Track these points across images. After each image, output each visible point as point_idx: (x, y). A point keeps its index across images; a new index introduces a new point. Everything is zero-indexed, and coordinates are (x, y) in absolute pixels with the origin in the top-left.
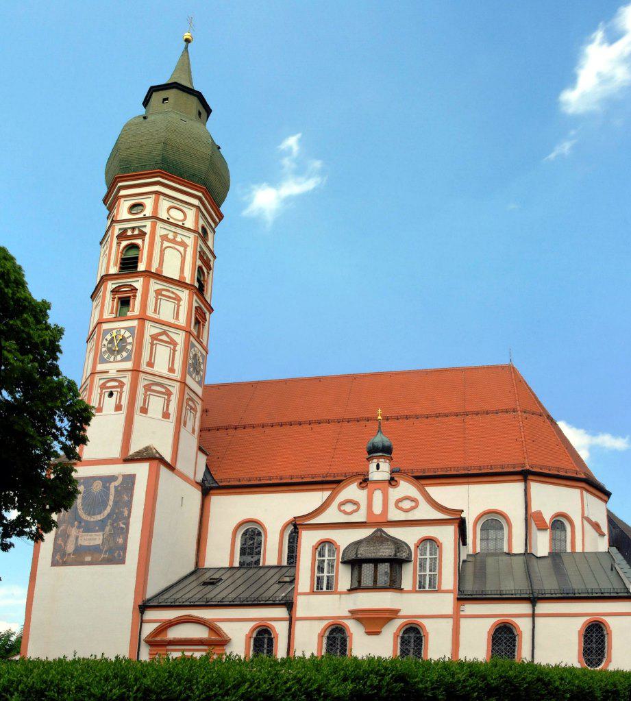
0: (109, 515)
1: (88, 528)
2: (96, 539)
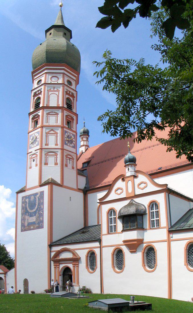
0: (37, 209)
1: (31, 216)
2: (33, 219)
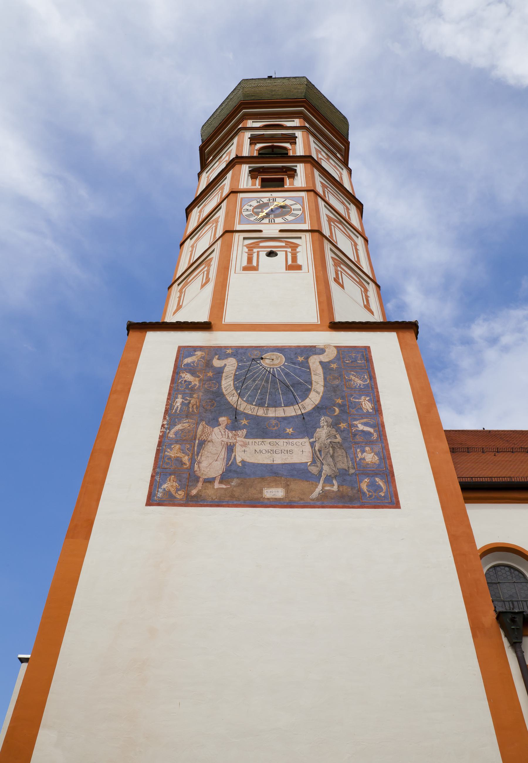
0: (318, 409)
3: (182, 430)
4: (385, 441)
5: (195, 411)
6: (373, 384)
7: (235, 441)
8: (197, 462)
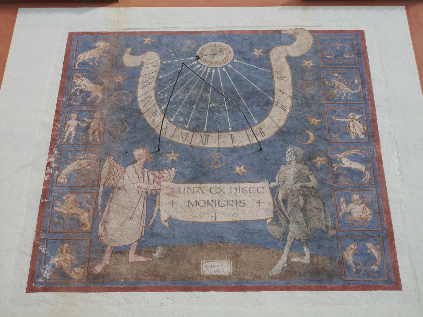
3: (78, 171)
4: (382, 184)
5: (98, 139)
6: (367, 93)
7: (159, 186)
8: (101, 222)
